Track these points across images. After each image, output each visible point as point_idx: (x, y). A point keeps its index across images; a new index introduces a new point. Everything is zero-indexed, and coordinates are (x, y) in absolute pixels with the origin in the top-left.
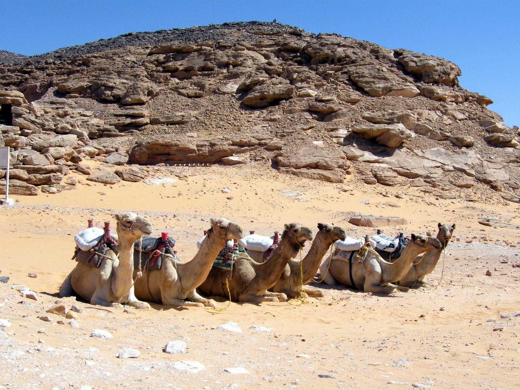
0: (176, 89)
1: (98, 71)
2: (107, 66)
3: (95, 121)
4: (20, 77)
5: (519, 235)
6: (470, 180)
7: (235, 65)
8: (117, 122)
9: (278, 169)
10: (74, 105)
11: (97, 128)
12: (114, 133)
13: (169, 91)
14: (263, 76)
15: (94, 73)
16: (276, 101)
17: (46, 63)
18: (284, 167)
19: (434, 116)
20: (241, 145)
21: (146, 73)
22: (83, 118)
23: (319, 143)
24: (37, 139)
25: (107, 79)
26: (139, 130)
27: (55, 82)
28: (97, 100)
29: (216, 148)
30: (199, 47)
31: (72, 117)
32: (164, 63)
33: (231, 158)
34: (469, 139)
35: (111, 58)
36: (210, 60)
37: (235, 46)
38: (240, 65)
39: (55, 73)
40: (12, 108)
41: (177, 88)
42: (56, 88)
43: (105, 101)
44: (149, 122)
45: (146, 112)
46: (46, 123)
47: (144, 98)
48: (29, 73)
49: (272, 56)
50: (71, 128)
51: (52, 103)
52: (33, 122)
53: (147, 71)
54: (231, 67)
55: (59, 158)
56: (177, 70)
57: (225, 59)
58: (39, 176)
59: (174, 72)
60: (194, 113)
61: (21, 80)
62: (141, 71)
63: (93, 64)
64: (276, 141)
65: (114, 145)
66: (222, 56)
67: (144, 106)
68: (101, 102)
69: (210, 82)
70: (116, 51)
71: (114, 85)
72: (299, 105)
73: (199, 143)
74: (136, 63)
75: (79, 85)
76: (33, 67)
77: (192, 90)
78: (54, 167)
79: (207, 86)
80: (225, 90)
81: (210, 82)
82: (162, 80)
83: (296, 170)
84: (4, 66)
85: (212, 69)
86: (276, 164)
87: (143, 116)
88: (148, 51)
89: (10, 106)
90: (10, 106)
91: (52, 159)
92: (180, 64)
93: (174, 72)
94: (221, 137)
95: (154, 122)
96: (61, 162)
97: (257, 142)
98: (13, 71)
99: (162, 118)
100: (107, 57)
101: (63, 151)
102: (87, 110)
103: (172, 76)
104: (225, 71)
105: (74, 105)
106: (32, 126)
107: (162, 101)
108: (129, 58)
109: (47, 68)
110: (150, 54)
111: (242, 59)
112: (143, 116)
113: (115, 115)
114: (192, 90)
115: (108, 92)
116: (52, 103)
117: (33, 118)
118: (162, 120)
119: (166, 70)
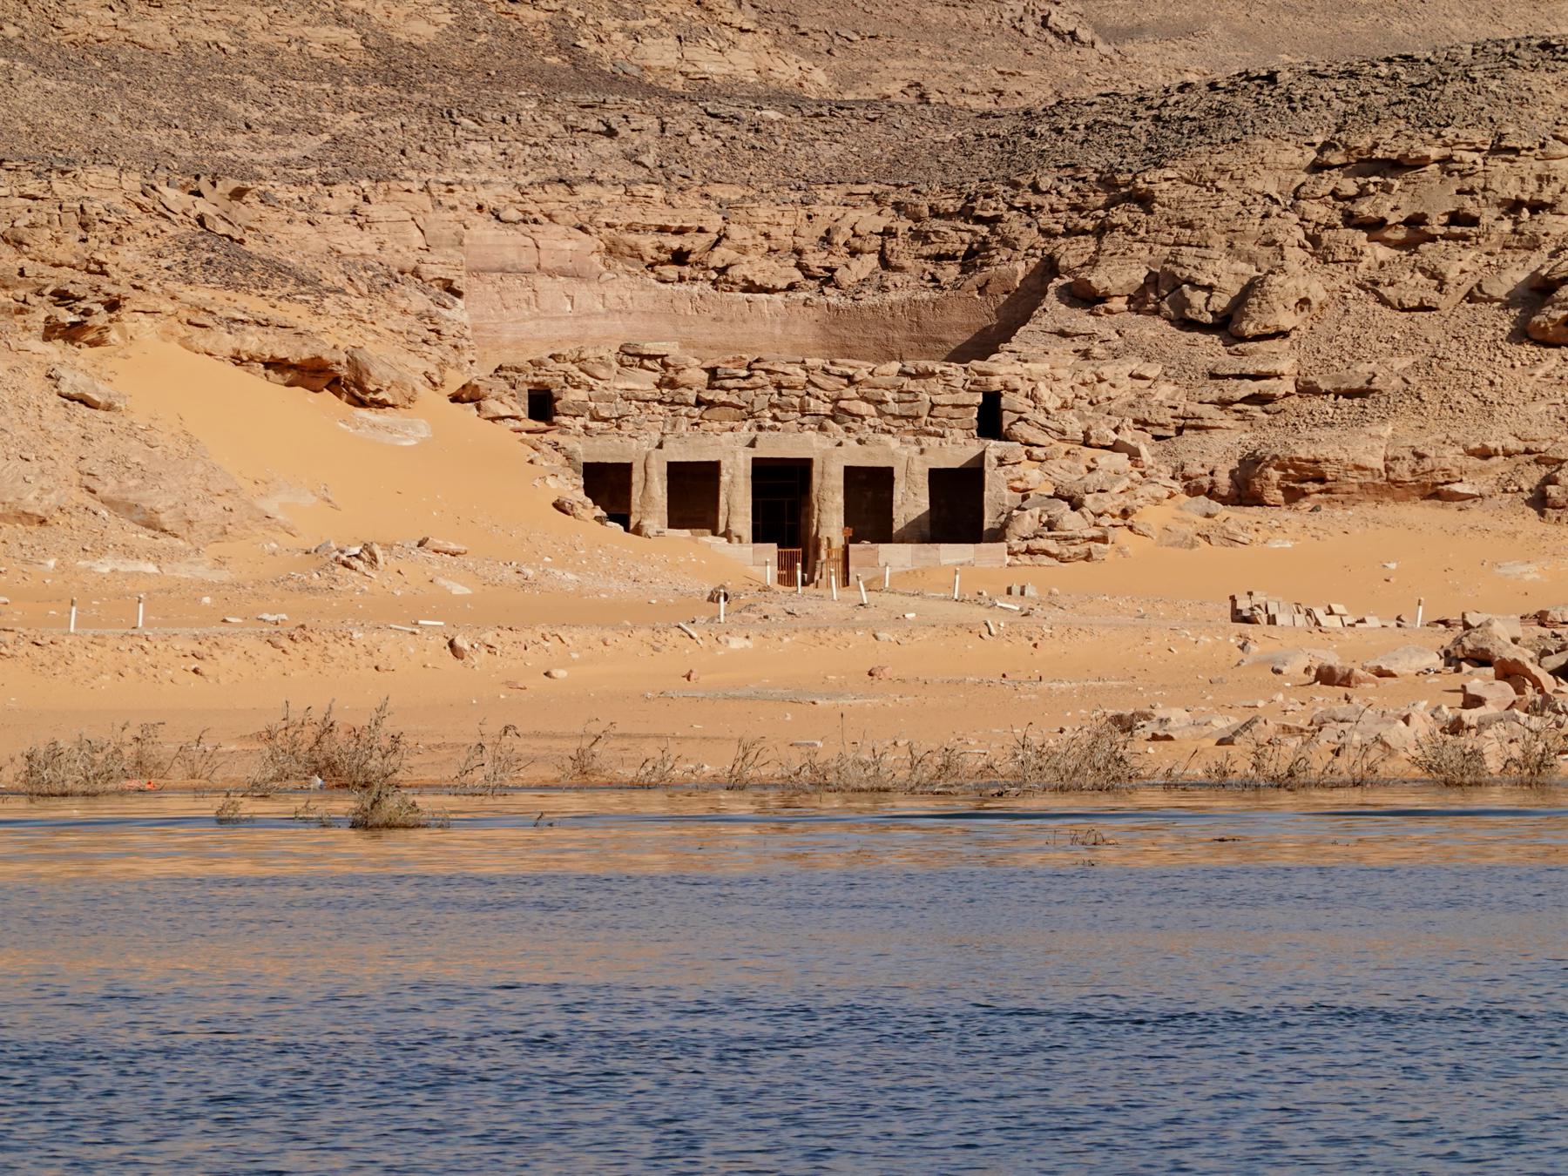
0: (1371, 286)
1: (1176, 230)
2: (1200, 214)
3: (1164, 391)
4: (967, 237)
7: (1536, 207)
8: (1216, 395)
9: (1542, 514)
10: (1118, 342)
11: (1172, 412)
12: (1208, 423)
13: (1355, 290)
15: (1163, 237)
17: (1035, 188)
18: (1554, 508)
20: (1485, 454)
21: (1300, 234)
22: (1141, 383)
24: (1058, 470)
25: (1196, 262)
26: (1266, 412)
27: (1063, 262)
28: (1171, 322)
29: (1427, 464)
30: (1447, 152)
31: (1113, 386)
32: (1352, 199)
33: (1457, 487)
35: (1213, 182)
36: (1472, 192)
37: (1542, 146)
38: (1550, 207)
39: (1060, 228)
40: (1003, 401)
41: (1376, 283)
42: (1068, 280)
44: (1293, 391)
45: (1286, 365)
46: (1068, 429)
47: (1286, 320)
48: (992, 222)
50: (1114, 437)
51: (1062, 334)
52: (1043, 428)
53: (1304, 228)
54: (1525, 213)
55: (1100, 515)
56: (1381, 223)
57: (1512, 190)
58: (1073, 549)
59: (1375, 227)
60: (1402, 363)
61: (971, 245)
62: (1290, 232)
63: (1163, 205)
65: (1210, 462)
66: (1508, 180)
67: (1287, 343)
68: (1181, 328)
69: (1461, 264)
70: (1223, 159)
71: (1214, 281)
73: (1390, 453)
74: (1277, 202)
75: (1126, 278)
76: (1002, 205)
77: (1413, 287)
78: (1095, 532)
79: (1452, 275)
80: (1495, 294)
81: (1460, 264)
82: (1341, 256)
84: (915, 191)
85: (1474, 221)
86: (1540, 501)
87: (1279, 376)
88: (1311, 154)
89: (998, 395)
90: (998, 395)
91: (1091, 518)
92: (1392, 204)
93: (1375, 227)
94: (1442, 437)
95: (1307, 389)
96: (1106, 521)
97: (1522, 447)
98: (947, 216)
99: (1325, 379)
100: (1201, 183)
101: (1111, 503)
102: (1148, 359)
103: (1369, 240)
104: (1507, 226)
105: (1118, 342)
106: (1042, 439)
107: (1332, 325)
108: (1258, 186)
109: (1040, 208)
110: (1317, 168)
111: (1556, 187)
112: (1279, 376)
113: (1213, 376)
114: (1413, 287)
115: (1198, 299)
116: (1062, 334)
117: (1042, 418)
118: (1323, 386)
119: (1351, 220)
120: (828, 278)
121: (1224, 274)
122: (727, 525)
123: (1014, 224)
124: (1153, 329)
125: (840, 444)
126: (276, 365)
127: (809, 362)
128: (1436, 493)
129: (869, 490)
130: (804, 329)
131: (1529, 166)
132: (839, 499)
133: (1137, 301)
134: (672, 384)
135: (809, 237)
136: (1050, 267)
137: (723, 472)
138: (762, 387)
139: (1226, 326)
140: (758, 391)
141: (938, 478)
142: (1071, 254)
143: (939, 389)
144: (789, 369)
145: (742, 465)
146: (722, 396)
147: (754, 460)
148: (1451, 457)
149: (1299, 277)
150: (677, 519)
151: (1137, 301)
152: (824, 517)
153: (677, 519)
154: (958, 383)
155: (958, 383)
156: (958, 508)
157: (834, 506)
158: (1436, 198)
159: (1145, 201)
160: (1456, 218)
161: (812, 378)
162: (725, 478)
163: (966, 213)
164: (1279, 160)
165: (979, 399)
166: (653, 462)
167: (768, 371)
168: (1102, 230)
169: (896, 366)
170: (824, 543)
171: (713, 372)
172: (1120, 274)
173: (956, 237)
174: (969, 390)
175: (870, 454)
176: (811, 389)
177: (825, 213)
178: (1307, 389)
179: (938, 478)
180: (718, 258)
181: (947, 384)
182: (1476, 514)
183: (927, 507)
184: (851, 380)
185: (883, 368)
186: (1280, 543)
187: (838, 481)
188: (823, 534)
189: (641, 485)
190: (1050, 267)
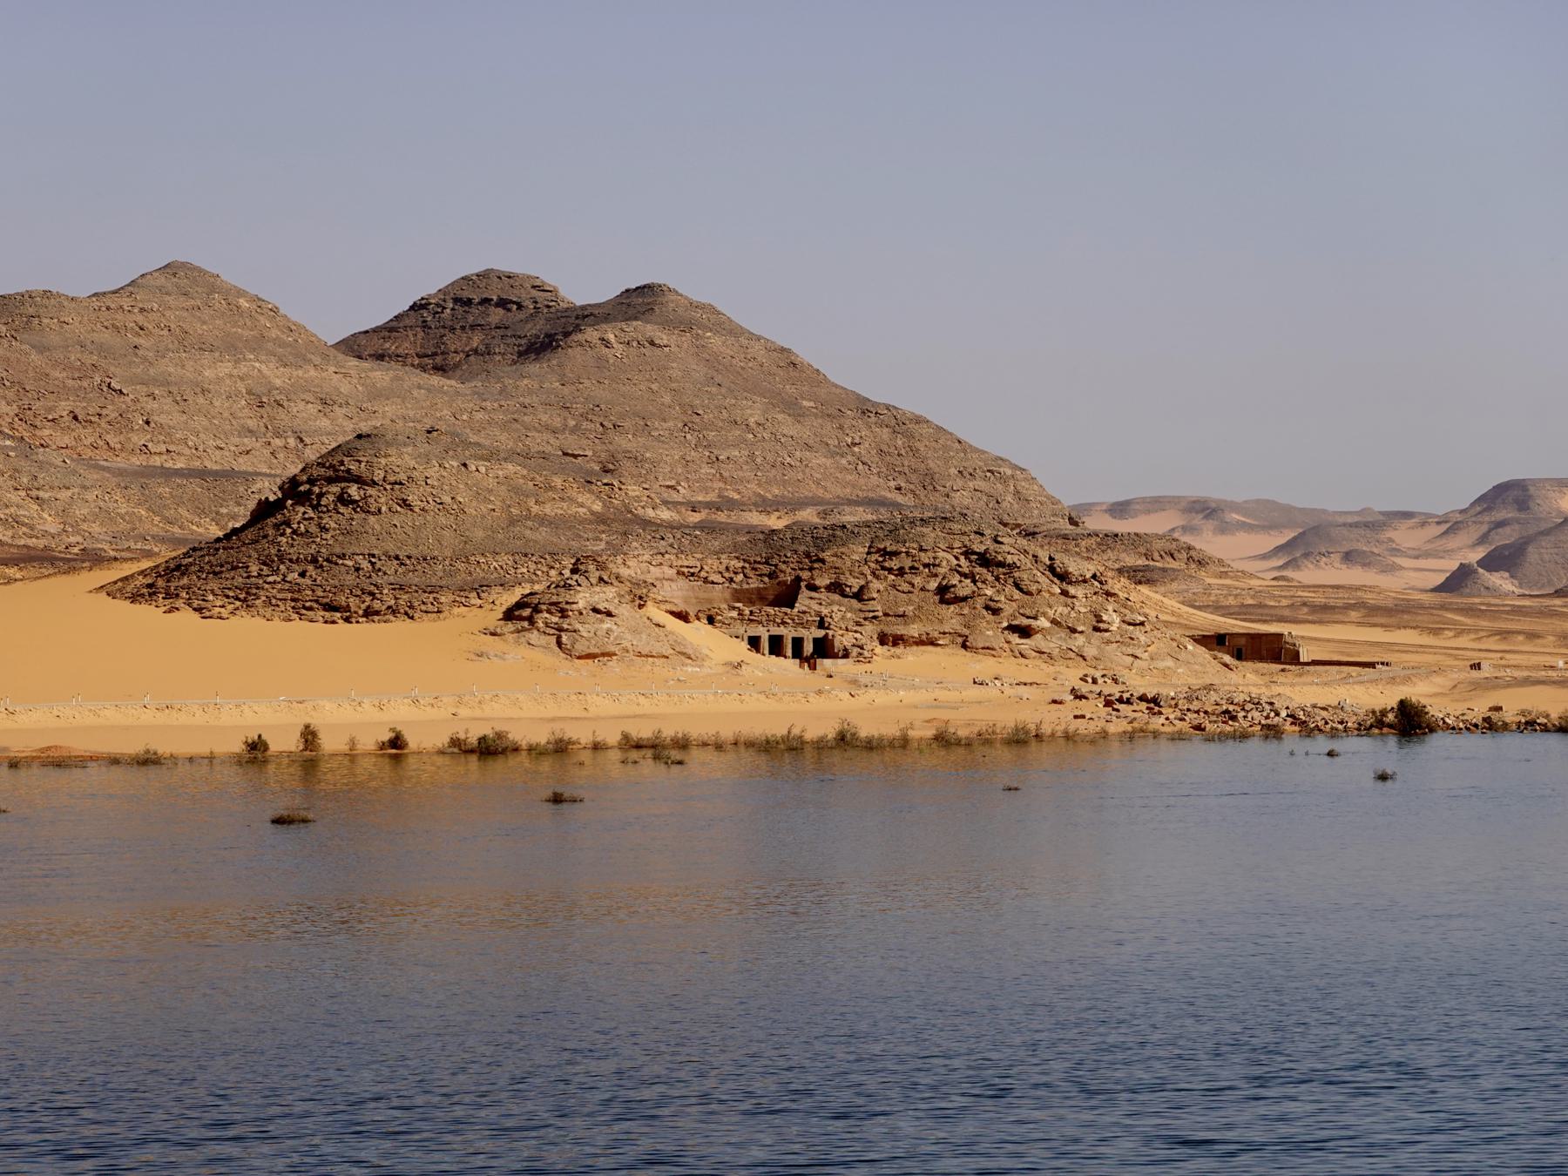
0: (894, 586)
5: (1553, 704)
6: (1072, 655)
14: (955, 580)
16: (964, 599)
19: (1066, 610)
23: (990, 633)
34: (1080, 629)
43: (844, 595)
49: (962, 558)
59: (890, 570)
64: (966, 631)
66: (925, 558)
72: (980, 602)
77: (906, 587)
81: (917, 581)
83: (974, 649)
86: (964, 646)
92: (894, 564)
93: (890, 570)
95: (886, 615)
119: (883, 568)
120: (731, 580)
121: (855, 583)
123: (783, 567)
124: (837, 597)
126: (672, 613)
128: (933, 643)
129: (798, 643)
130: (727, 595)
131: (930, 554)
133: (829, 588)
135: (722, 568)
136: (798, 579)
139: (859, 596)
141: (815, 640)
142: (805, 575)
148: (936, 634)
149: (876, 585)
150: (771, 653)
151: (829, 588)
153: (771, 653)
156: (824, 648)
158: (908, 563)
159: (823, 561)
160: (912, 568)
163: (767, 563)
164: (858, 551)
168: (811, 569)
172: (823, 581)
173: (765, 569)
177: (725, 562)
178: (886, 615)
179: (815, 640)
180: (703, 574)
182: (947, 650)
186: (910, 658)
190: (798, 579)
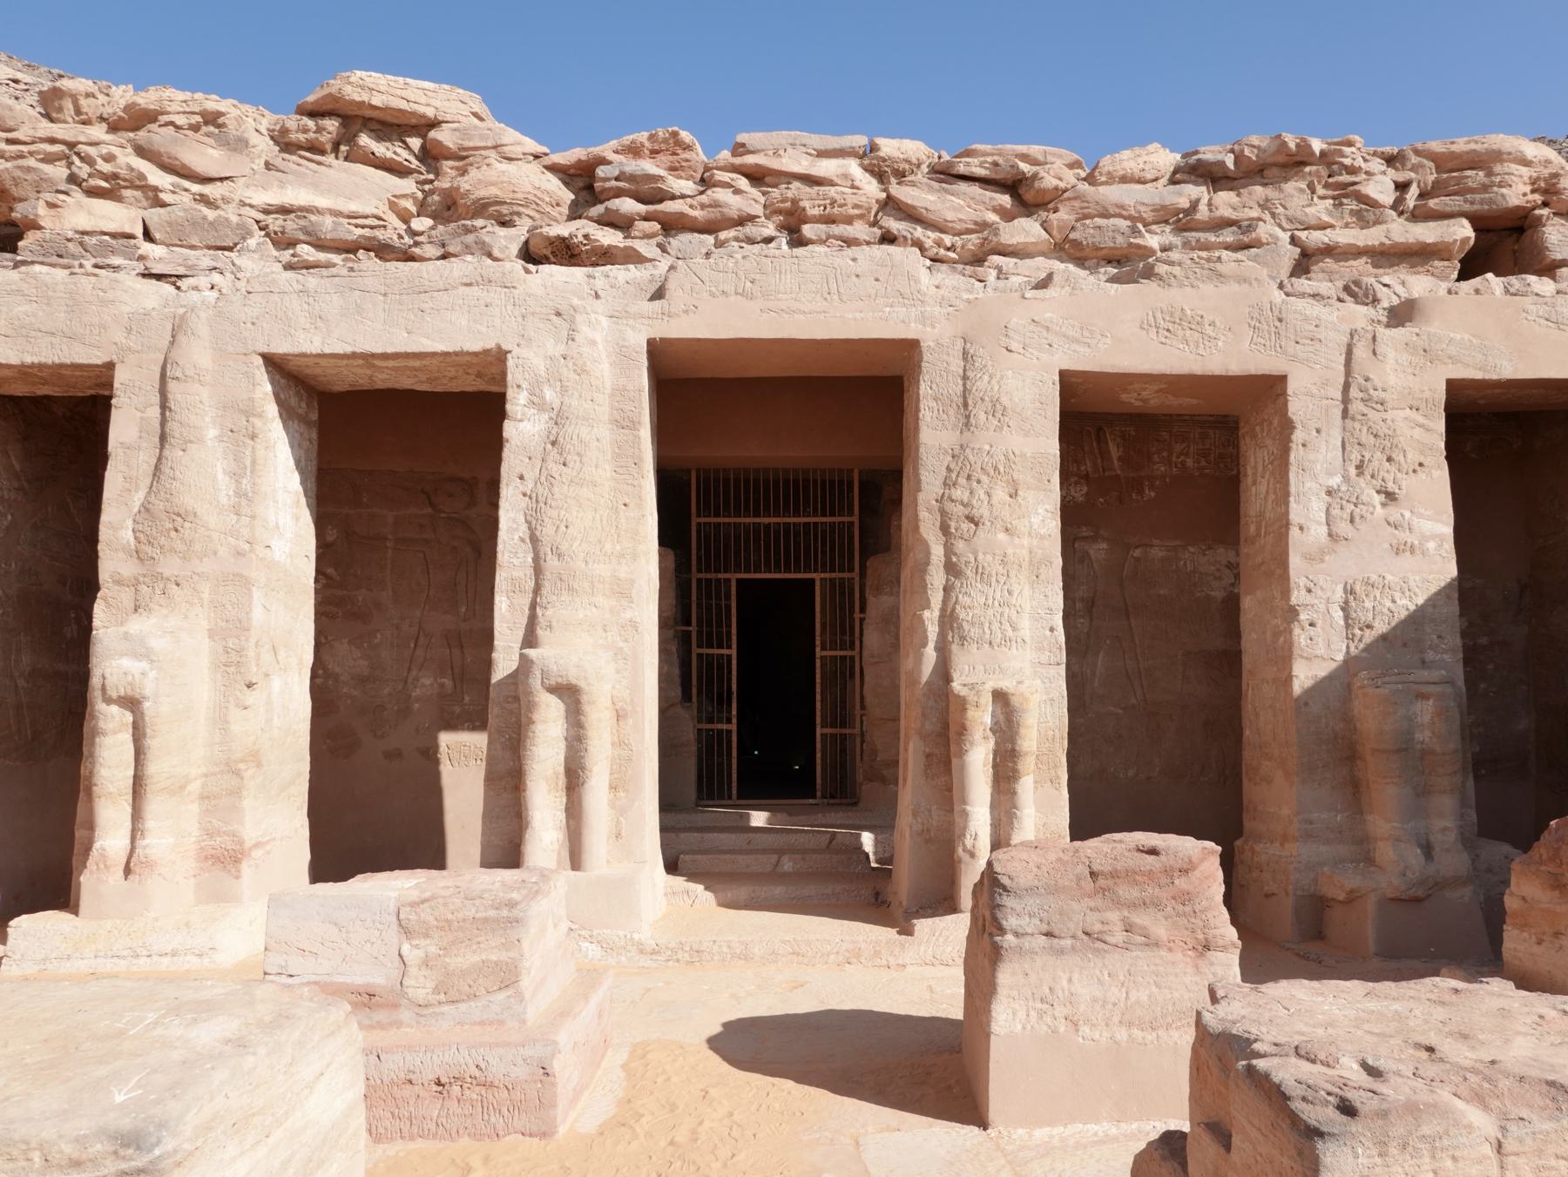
122: (530, 640)
125: (1043, 284)
127: (890, 147)
132: (1036, 518)
134: (449, 209)
137: (517, 402)
138: (744, 220)
140: (723, 235)
143: (1321, 209)
144: (826, 168)
145: (604, 371)
146: (609, 238)
147: (657, 351)
152: (973, 602)
154: (1380, 188)
155: (1380, 188)
157: (1019, 548)
161: (897, 190)
162: (523, 429)
165: (1463, 231)
166: (198, 354)
167: (757, 177)
169: (1165, 159)
170: (982, 718)
171: (584, 183)
174: (1418, 216)
175: (1175, 323)
176: (895, 225)
181: (1345, 192)
183: (1446, 568)
184: (1020, 192)
185: (1127, 160)
187: (1037, 442)
188: (972, 676)
189: (145, 459)
